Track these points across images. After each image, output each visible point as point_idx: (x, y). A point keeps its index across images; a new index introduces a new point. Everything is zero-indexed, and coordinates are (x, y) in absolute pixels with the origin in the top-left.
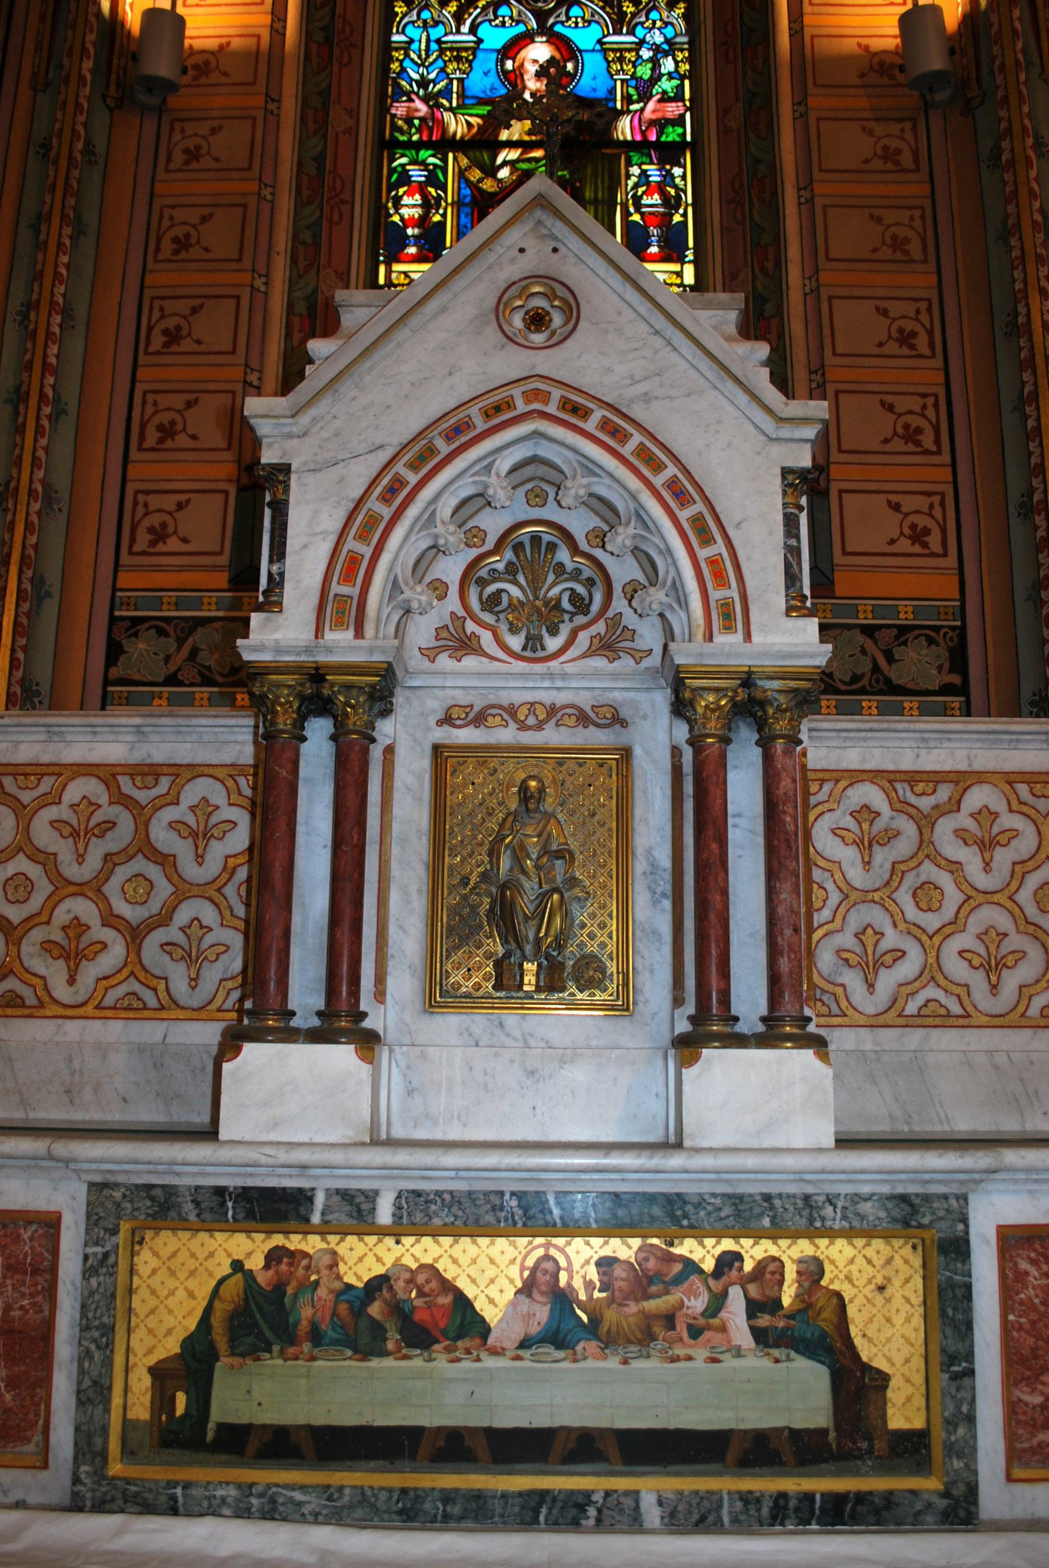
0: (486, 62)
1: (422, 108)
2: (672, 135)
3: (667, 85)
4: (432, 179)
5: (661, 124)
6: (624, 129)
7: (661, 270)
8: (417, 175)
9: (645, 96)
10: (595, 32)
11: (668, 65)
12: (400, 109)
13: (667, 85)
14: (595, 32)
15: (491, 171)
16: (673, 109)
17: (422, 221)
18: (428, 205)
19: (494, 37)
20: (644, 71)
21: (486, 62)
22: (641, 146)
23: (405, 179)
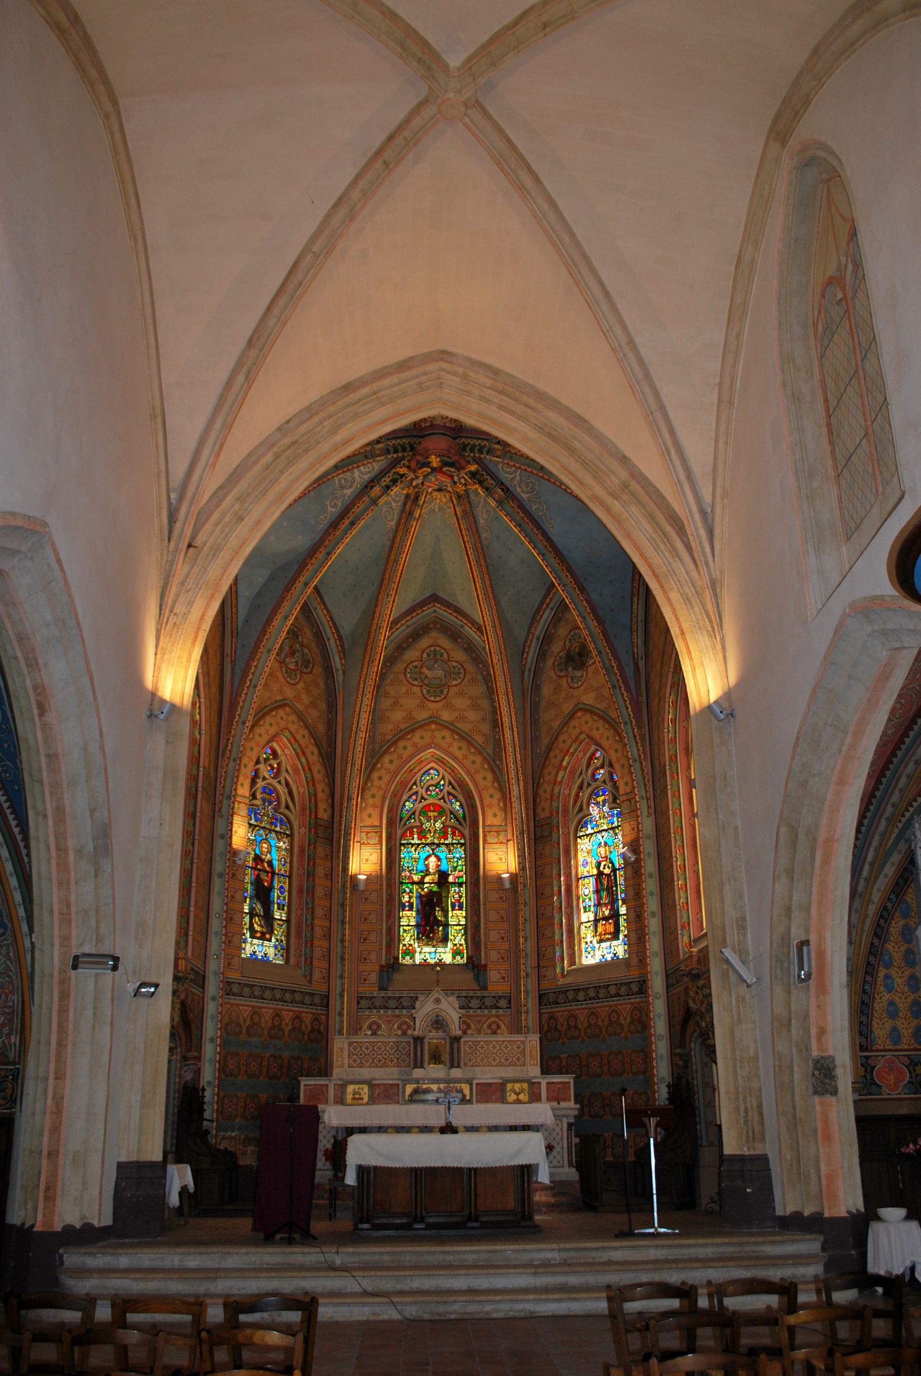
0: (421, 861)
1: (408, 874)
2: (461, 880)
3: (459, 868)
4: (411, 892)
5: (458, 877)
6: (451, 879)
7: (458, 912)
8: (408, 890)
9: (455, 870)
10: (444, 854)
11: (460, 863)
12: (403, 874)
13: (459, 868)
14: (444, 854)
15: (423, 889)
16: (461, 874)
17: (409, 902)
18: (410, 898)
19: (423, 856)
20: (455, 864)
21: (421, 861)
22: (454, 883)
23: (405, 891)
